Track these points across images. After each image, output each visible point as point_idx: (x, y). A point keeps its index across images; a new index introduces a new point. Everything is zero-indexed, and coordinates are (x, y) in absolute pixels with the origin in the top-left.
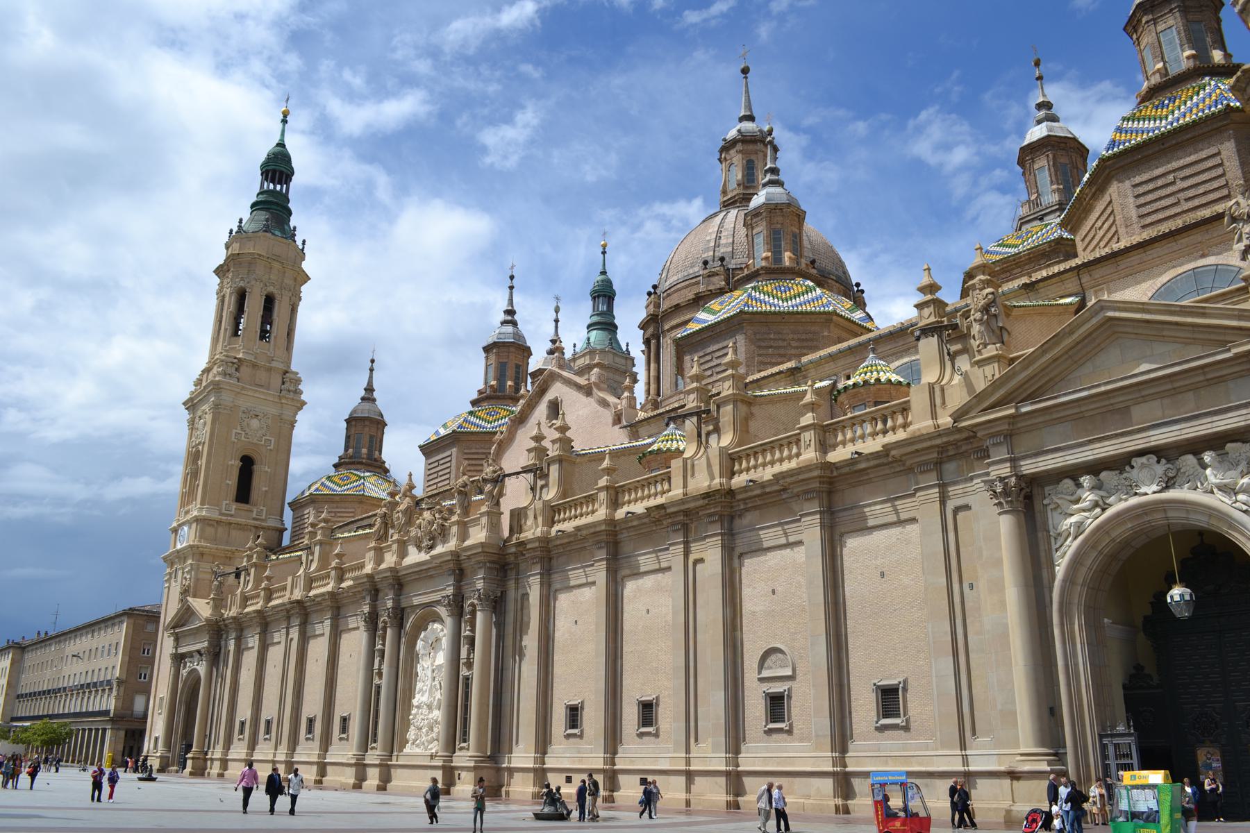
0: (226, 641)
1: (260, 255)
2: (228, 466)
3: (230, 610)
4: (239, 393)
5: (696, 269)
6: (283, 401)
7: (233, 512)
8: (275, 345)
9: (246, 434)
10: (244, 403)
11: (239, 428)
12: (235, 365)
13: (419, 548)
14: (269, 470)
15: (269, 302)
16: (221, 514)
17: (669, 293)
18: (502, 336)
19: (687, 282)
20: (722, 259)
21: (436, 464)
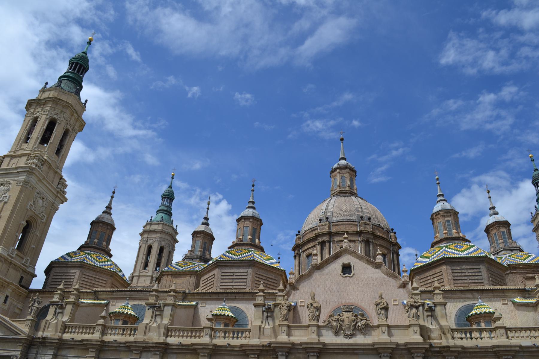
0: (37, 354)
1: (72, 106)
2: (20, 224)
3: (43, 331)
4: (40, 180)
5: (354, 218)
6: (59, 195)
7: (14, 256)
8: (61, 160)
9: (35, 207)
10: (40, 188)
11: (32, 202)
12: (43, 163)
13: (337, 334)
14: (39, 235)
15: (66, 133)
16: (8, 255)
17: (337, 223)
18: (254, 214)
19: (350, 223)
20: (369, 219)
21: (232, 274)
